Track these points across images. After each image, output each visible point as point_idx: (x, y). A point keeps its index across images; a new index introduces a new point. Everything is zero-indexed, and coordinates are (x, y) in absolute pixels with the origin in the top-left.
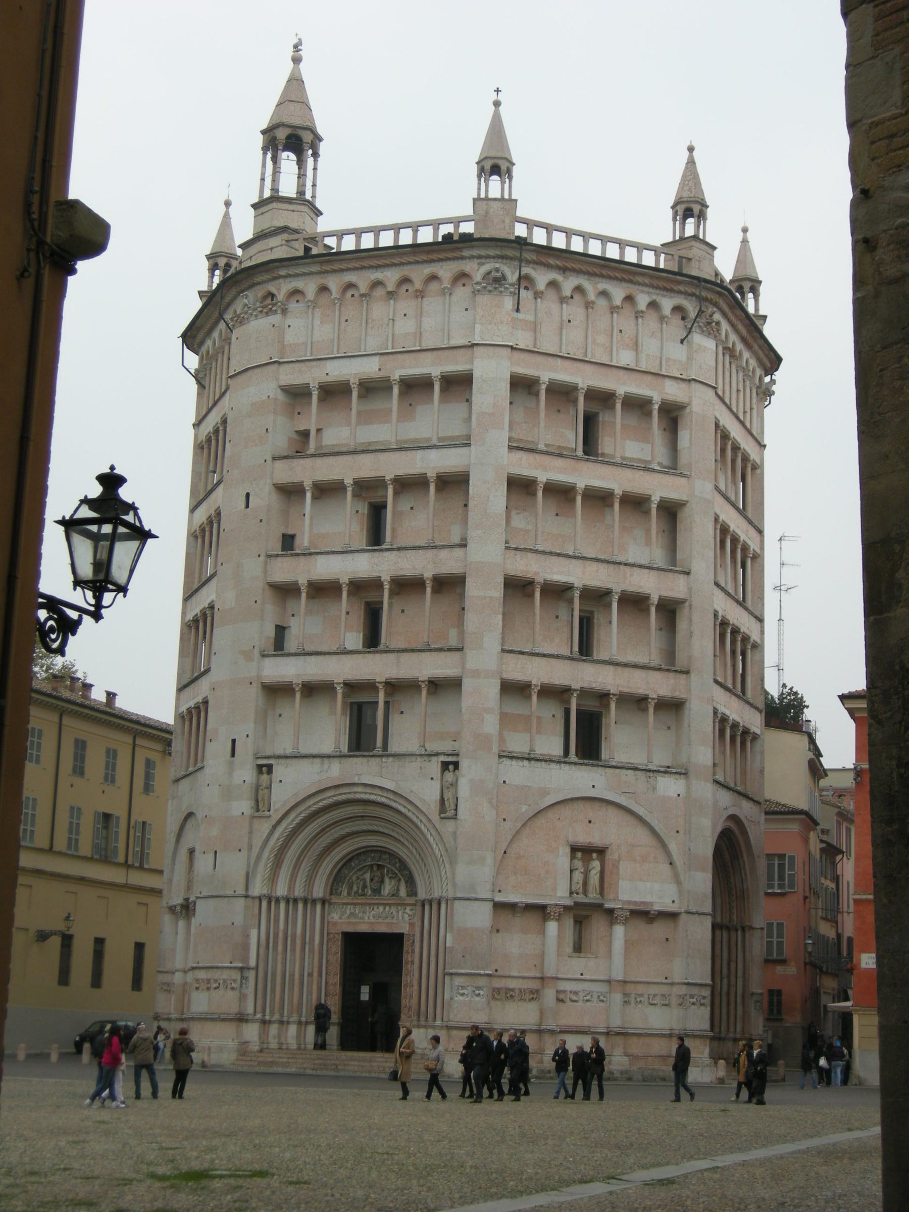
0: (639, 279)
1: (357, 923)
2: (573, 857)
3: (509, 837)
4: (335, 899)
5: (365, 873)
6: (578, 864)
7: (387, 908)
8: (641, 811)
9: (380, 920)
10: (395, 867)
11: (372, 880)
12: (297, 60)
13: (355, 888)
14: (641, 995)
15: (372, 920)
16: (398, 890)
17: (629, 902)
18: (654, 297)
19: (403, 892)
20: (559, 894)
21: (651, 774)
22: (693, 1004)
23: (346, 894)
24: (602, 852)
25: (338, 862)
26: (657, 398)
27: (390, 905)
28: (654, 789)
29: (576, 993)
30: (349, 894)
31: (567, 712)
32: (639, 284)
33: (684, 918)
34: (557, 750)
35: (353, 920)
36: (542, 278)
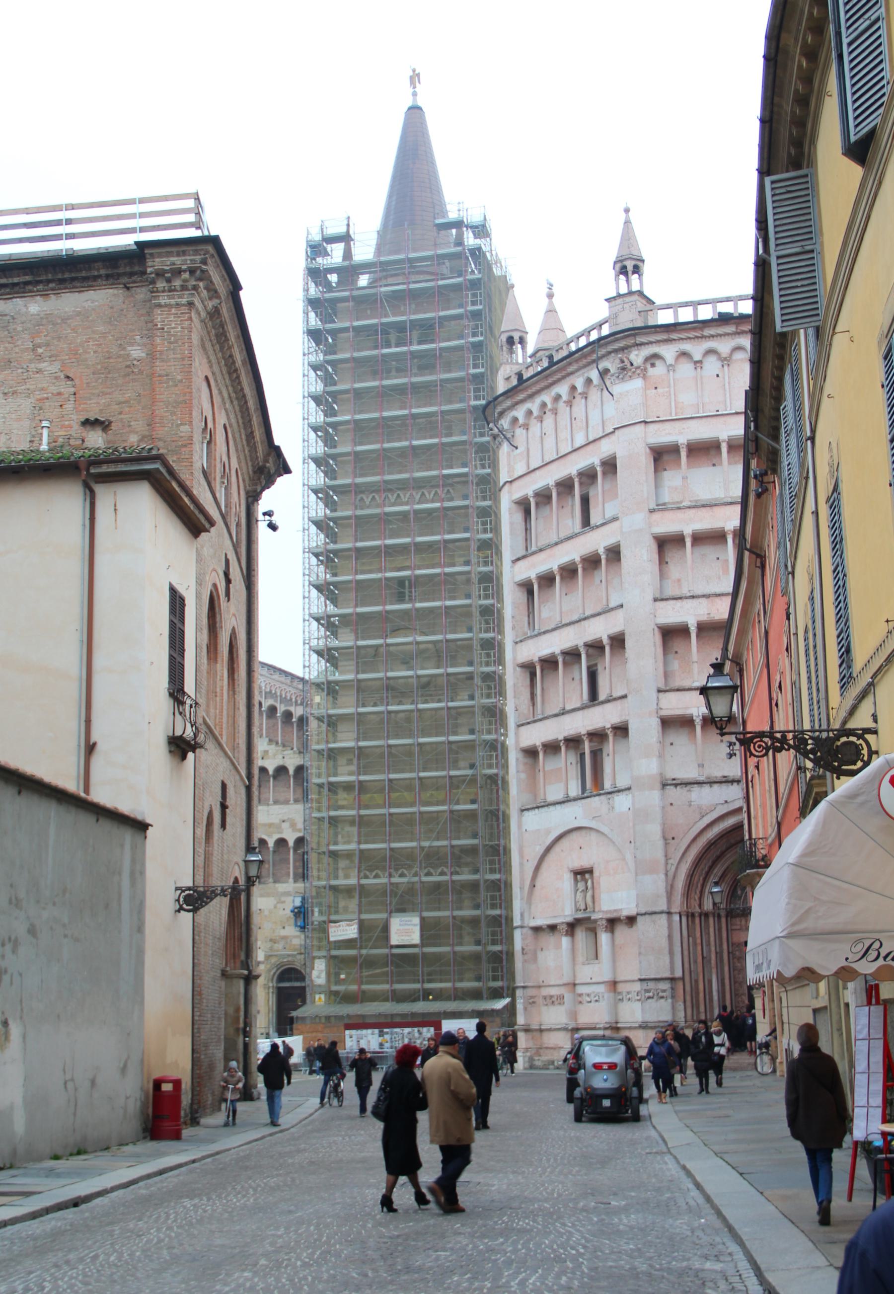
0: (571, 369)
2: (576, 881)
3: (531, 874)
6: (581, 886)
8: (604, 829)
12: (550, 296)
14: (628, 993)
17: (607, 912)
18: (586, 375)
20: (566, 913)
21: (609, 796)
22: (649, 998)
24: (590, 871)
26: (597, 462)
28: (613, 808)
29: (588, 995)
31: (582, 755)
32: (572, 373)
33: (639, 918)
34: (574, 790)
36: (519, 413)
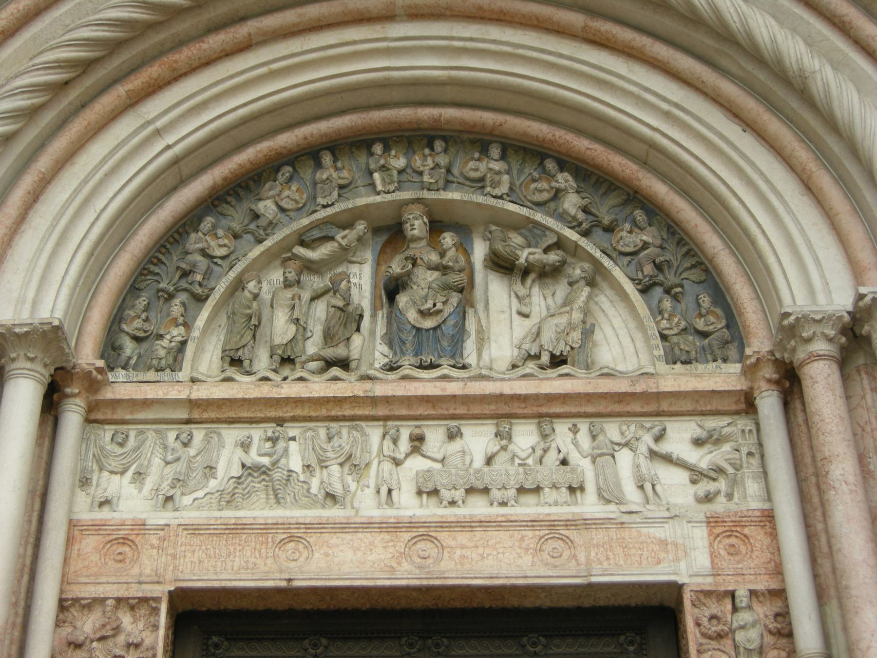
1: (294, 534)
4: (123, 386)
5: (345, 255)
7: (525, 436)
9: (478, 508)
10: (562, 217)
11: (392, 289)
13: (281, 328)
15: (409, 505)
16: (588, 333)
19: (623, 342)
23: (206, 358)
25: (177, 172)
27: (543, 411)
30: (235, 361)
35: (259, 510)
